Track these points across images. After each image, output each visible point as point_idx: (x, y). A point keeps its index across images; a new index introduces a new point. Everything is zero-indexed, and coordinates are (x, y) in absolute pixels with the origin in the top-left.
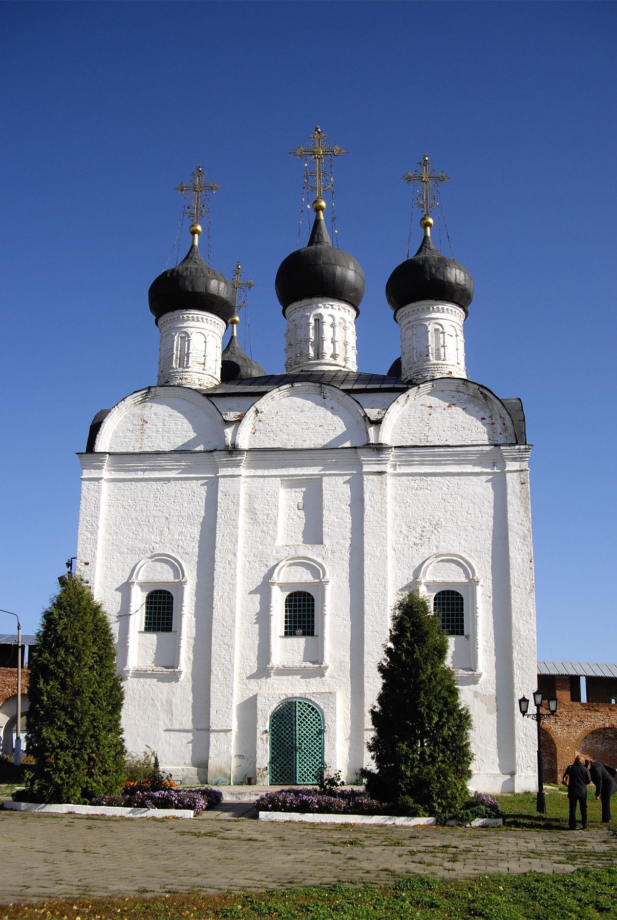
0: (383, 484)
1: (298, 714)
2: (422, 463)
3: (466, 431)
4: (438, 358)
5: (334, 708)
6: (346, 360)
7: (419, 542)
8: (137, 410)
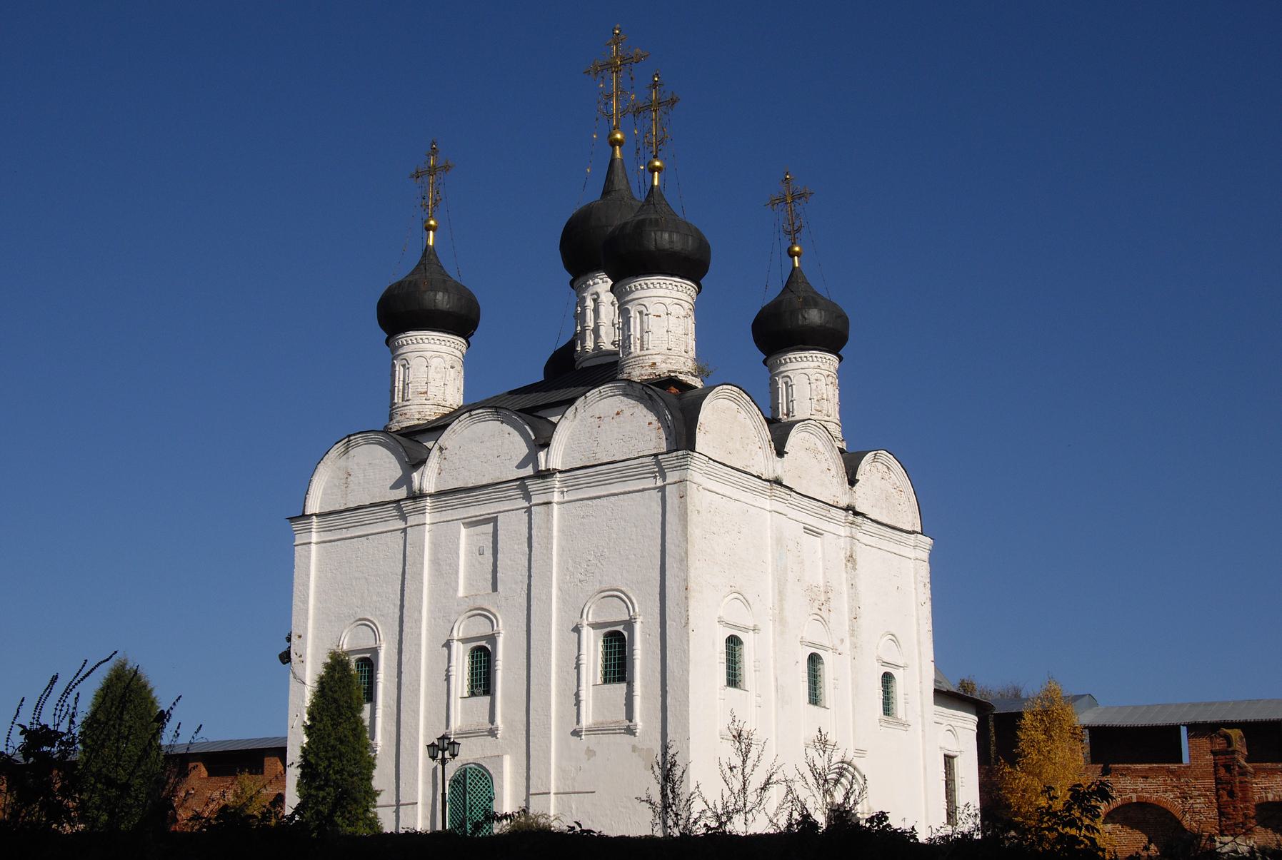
0: (549, 515)
1: (468, 781)
2: (589, 486)
3: (634, 442)
4: (642, 349)
5: (502, 773)
7: (583, 578)
8: (342, 462)
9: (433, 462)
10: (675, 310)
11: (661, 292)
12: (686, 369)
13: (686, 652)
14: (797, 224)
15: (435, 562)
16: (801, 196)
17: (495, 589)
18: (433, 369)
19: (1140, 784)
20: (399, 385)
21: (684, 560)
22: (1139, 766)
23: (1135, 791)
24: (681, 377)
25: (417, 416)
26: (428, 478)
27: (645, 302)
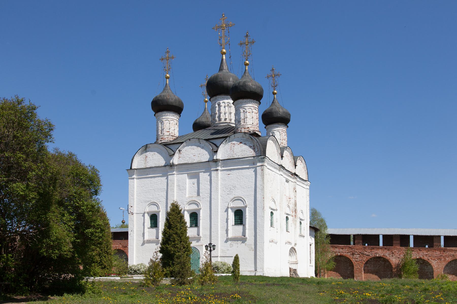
4: (244, 122)
6: (230, 120)
7: (229, 193)
9: (177, 155)
10: (254, 111)
11: (250, 105)
12: (257, 130)
13: (263, 217)
14: (276, 84)
15: (178, 186)
16: (277, 75)
17: (198, 194)
18: (171, 126)
19: (341, 250)
20: (160, 129)
21: (263, 189)
22: (341, 245)
23: (339, 252)
24: (257, 132)
25: (167, 139)
26: (176, 160)
27: (246, 108)
